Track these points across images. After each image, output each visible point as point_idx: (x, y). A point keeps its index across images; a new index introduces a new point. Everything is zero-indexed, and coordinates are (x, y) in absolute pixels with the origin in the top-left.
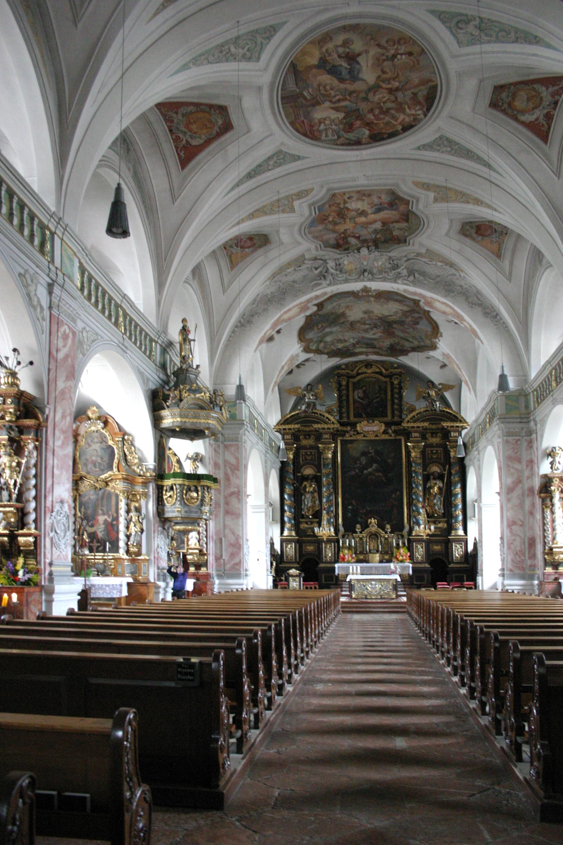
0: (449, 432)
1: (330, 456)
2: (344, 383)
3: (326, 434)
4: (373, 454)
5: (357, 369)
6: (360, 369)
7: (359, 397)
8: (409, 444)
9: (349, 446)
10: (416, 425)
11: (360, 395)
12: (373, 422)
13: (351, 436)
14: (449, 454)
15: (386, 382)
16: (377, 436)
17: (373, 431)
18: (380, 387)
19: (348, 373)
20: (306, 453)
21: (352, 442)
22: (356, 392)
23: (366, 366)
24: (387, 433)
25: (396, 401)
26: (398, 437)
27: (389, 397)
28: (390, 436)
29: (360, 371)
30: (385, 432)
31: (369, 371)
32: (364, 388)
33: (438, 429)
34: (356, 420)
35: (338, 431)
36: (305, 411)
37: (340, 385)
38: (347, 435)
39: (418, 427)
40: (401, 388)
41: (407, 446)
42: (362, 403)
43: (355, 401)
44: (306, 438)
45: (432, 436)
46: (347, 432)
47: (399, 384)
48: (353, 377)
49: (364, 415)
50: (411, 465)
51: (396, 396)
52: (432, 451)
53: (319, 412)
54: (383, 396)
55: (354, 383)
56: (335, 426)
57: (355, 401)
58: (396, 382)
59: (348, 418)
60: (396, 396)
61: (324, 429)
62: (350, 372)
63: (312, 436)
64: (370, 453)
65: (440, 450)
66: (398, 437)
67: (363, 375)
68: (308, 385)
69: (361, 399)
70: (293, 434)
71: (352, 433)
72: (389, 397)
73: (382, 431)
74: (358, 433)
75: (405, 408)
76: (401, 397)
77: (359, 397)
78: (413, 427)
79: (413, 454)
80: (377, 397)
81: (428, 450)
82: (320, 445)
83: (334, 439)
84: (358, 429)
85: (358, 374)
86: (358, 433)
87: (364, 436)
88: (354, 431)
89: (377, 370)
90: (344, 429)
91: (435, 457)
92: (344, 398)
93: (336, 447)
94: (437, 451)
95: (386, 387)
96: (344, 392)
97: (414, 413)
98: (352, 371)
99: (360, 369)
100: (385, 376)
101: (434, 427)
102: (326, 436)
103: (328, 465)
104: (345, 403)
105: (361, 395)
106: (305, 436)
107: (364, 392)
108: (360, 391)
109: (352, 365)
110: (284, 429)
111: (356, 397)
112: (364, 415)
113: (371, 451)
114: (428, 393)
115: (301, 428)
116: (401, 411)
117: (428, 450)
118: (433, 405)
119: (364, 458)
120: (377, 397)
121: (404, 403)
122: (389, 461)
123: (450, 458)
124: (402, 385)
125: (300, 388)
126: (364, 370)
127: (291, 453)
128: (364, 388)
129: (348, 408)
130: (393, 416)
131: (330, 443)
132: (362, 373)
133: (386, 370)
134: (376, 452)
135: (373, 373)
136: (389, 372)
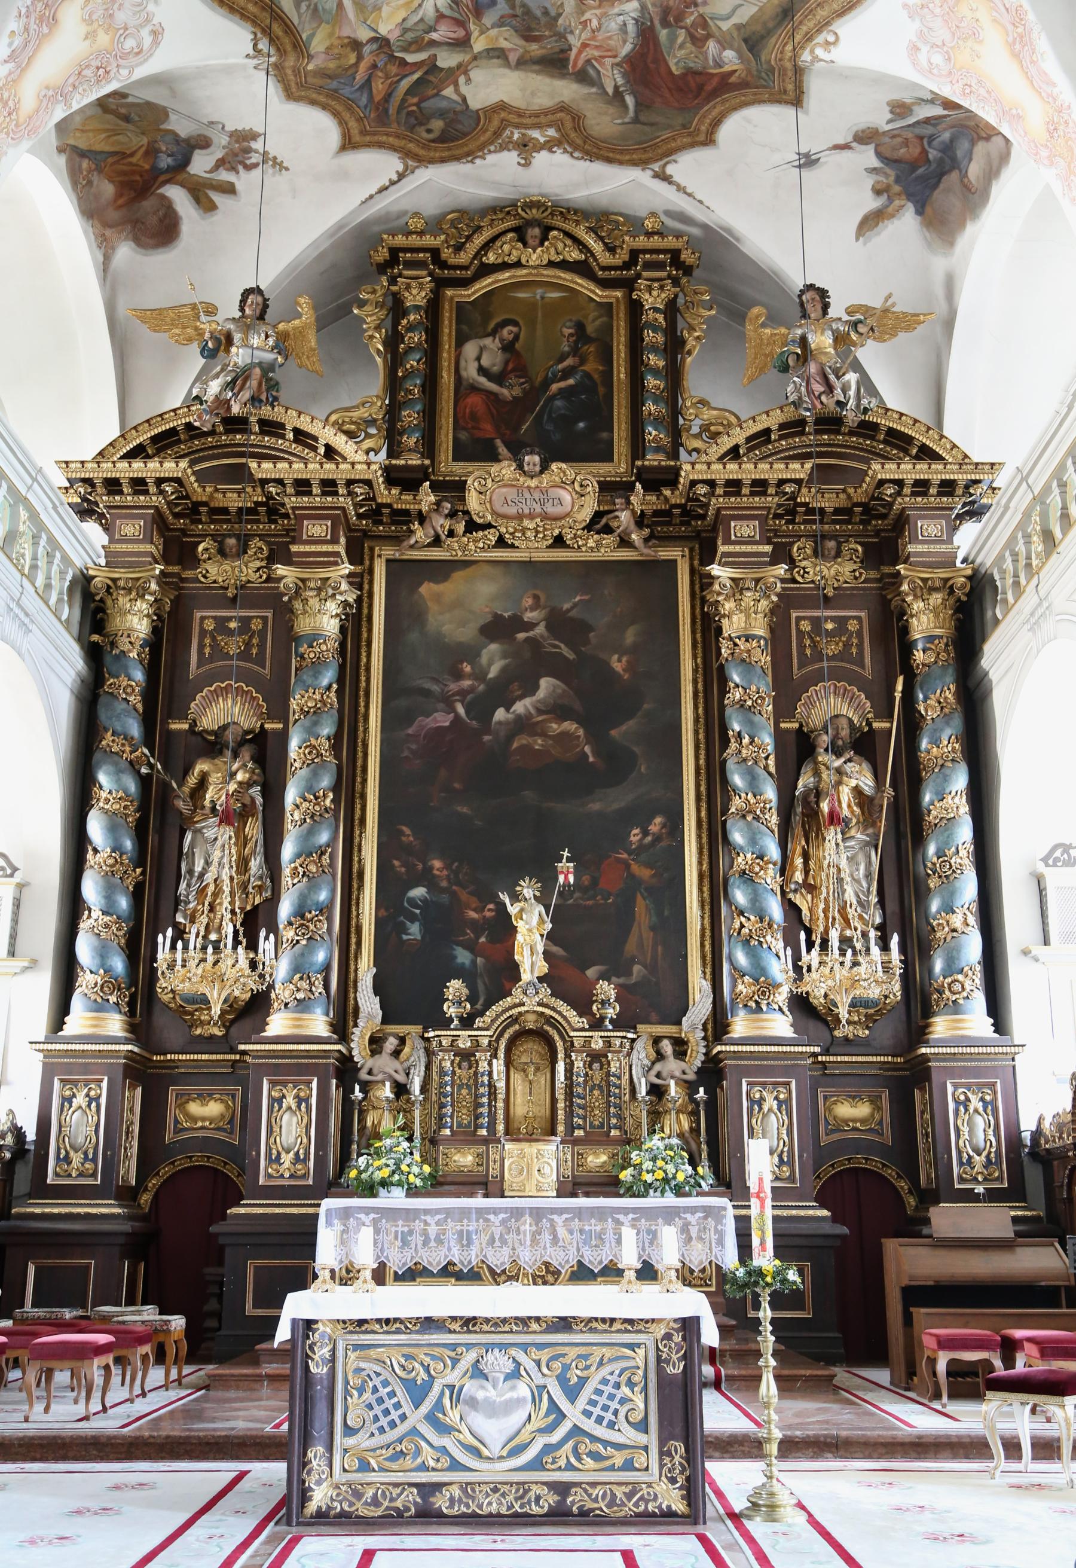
0: (901, 523)
1: (330, 626)
2: (416, 296)
3: (317, 514)
4: (540, 630)
5: (479, 240)
6: (487, 246)
7: (482, 370)
8: (715, 570)
9: (426, 589)
10: (747, 471)
11: (485, 362)
12: (544, 467)
13: (437, 542)
14: (905, 630)
15: (607, 308)
16: (559, 542)
17: (545, 517)
18: (580, 327)
19: (435, 252)
20: (221, 622)
21: (442, 570)
22: (470, 349)
23: (520, 234)
24: (608, 530)
25: (652, 382)
26: (666, 553)
27: (621, 373)
28: (625, 542)
29: (491, 258)
30: (599, 523)
31: (535, 257)
32: (507, 332)
33: (844, 513)
34: (470, 466)
35: (375, 513)
36: (221, 403)
37: (397, 308)
38: (420, 534)
39: (760, 486)
40: (675, 346)
41: (702, 583)
42: (495, 395)
43: (463, 388)
44: (222, 552)
45: (818, 553)
46: (422, 518)
47: (671, 309)
48: (465, 283)
49: (502, 450)
50: (723, 680)
51: (655, 360)
52: (816, 623)
53: (291, 420)
54: (592, 366)
55: (461, 308)
56: (361, 471)
57: (463, 388)
58: (653, 299)
59: (429, 447)
60: (655, 360)
61: (302, 486)
62: (446, 254)
63: (255, 543)
64: (530, 626)
65: (858, 618)
66: (666, 553)
67: (505, 277)
68: (247, 293)
69: (499, 378)
70: (159, 521)
71: (441, 523)
72: (621, 373)
73: (586, 514)
74: (472, 527)
75: (694, 420)
76: (674, 376)
77: (482, 370)
78: (734, 486)
79: (732, 626)
80: (566, 374)
81: (801, 619)
82: (281, 570)
83: (355, 554)
84: (473, 502)
85: (487, 270)
86: (472, 527)
87: (501, 542)
88: (452, 515)
89: (574, 255)
90: (407, 502)
91: (832, 649)
92: (412, 363)
93: (364, 601)
94: (841, 622)
95: (607, 330)
96: (416, 337)
97: (738, 436)
98: (459, 248)
99: (487, 246)
100: (605, 284)
101: (828, 502)
102: (317, 529)
103: (318, 664)
104: (414, 386)
105: (493, 359)
106: (219, 539)
107: (508, 347)
108: (488, 341)
109: (453, 224)
110: (113, 485)
111: (470, 371)
112: (502, 450)
113: (529, 616)
114: (803, 341)
115: (199, 491)
116: (676, 434)
117: (801, 619)
118: (830, 389)
119: (494, 647)
120: (566, 374)
121: (687, 403)
122: (618, 664)
123: (907, 647)
124: (681, 324)
125: (211, 310)
126: (508, 249)
127: (142, 606)
128: (507, 332)
129: (430, 415)
130: (638, 447)
131: (332, 560)
132: (505, 266)
133: (611, 249)
134: (557, 623)
135: (551, 264)
136: (623, 256)
